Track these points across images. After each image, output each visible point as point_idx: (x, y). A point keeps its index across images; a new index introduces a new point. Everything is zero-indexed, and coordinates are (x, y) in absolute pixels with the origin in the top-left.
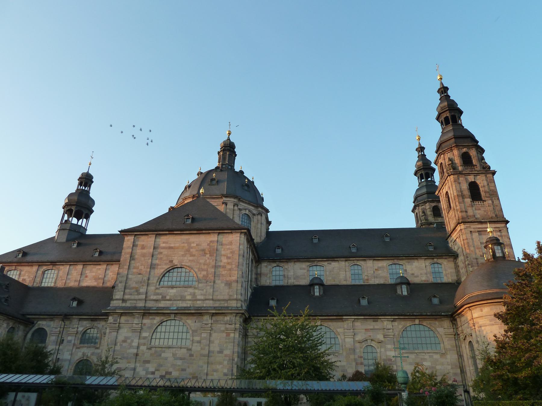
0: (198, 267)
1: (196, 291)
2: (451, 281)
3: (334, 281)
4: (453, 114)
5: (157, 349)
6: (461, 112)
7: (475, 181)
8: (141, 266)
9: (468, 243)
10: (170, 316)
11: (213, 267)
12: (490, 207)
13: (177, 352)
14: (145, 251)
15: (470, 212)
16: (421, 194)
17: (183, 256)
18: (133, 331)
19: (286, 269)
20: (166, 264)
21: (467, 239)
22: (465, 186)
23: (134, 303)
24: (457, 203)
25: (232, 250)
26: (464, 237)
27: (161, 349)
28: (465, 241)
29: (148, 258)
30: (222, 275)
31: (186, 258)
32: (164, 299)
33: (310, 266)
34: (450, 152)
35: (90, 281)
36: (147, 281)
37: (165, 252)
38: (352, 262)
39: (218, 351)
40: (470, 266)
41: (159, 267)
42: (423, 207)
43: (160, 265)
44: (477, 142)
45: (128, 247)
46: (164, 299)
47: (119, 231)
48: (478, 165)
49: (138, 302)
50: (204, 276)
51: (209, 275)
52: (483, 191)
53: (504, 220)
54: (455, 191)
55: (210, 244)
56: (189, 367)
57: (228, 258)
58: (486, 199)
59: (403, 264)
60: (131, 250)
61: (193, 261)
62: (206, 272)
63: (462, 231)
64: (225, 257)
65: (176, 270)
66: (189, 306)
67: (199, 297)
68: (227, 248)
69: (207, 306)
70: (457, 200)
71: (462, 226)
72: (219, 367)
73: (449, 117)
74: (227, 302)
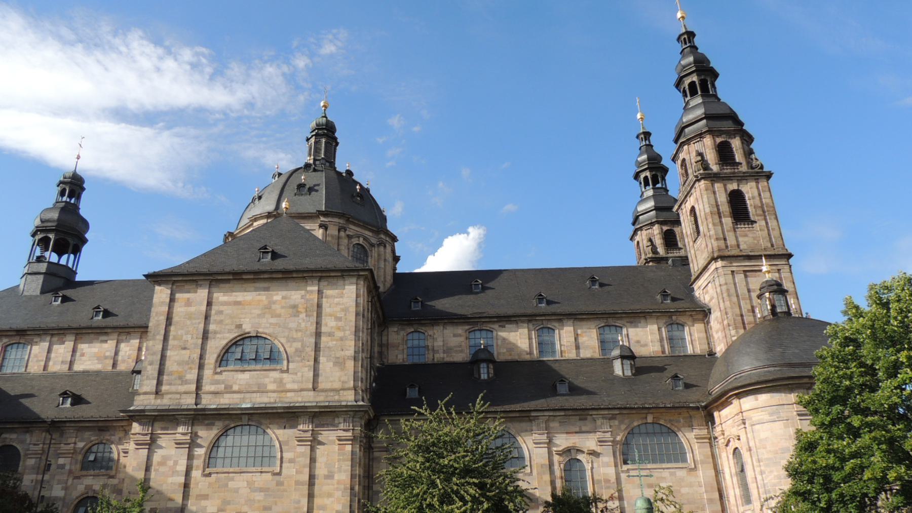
0: (286, 334)
1: (285, 375)
2: (699, 352)
3: (511, 355)
4: (703, 77)
5: (219, 475)
6: (715, 75)
7: (740, 188)
8: (186, 334)
9: (728, 290)
10: (241, 419)
11: (312, 336)
12: (763, 232)
13: (254, 479)
14: (192, 309)
17: (259, 316)
18: (178, 446)
19: (430, 336)
20: (230, 331)
21: (726, 284)
22: (723, 198)
23: (177, 399)
24: (711, 226)
25: (343, 306)
27: (226, 475)
28: (724, 288)
29: (197, 321)
30: (328, 347)
31: (264, 320)
32: (229, 390)
33: (470, 330)
34: (698, 141)
35: (89, 363)
36: (197, 361)
37: (227, 310)
38: (540, 323)
39: (325, 475)
40: (731, 328)
41: (218, 336)
42: (650, 231)
43: (220, 333)
44: (742, 124)
45: (163, 303)
46: (229, 390)
47: (144, 275)
48: (744, 163)
49: (184, 396)
50: (297, 350)
51: (306, 348)
52: (751, 205)
53: (785, 252)
54: (707, 206)
55: (306, 295)
56: (276, 504)
57: (338, 319)
58: (756, 218)
59: (621, 325)
60: (167, 308)
61: (276, 324)
62: (300, 344)
63: (719, 271)
64: (333, 318)
65: (247, 342)
66: (272, 400)
67: (289, 386)
68: (335, 302)
69: (304, 400)
70: (710, 220)
71: (720, 263)
72: (327, 501)
73: (697, 83)
74: (339, 393)
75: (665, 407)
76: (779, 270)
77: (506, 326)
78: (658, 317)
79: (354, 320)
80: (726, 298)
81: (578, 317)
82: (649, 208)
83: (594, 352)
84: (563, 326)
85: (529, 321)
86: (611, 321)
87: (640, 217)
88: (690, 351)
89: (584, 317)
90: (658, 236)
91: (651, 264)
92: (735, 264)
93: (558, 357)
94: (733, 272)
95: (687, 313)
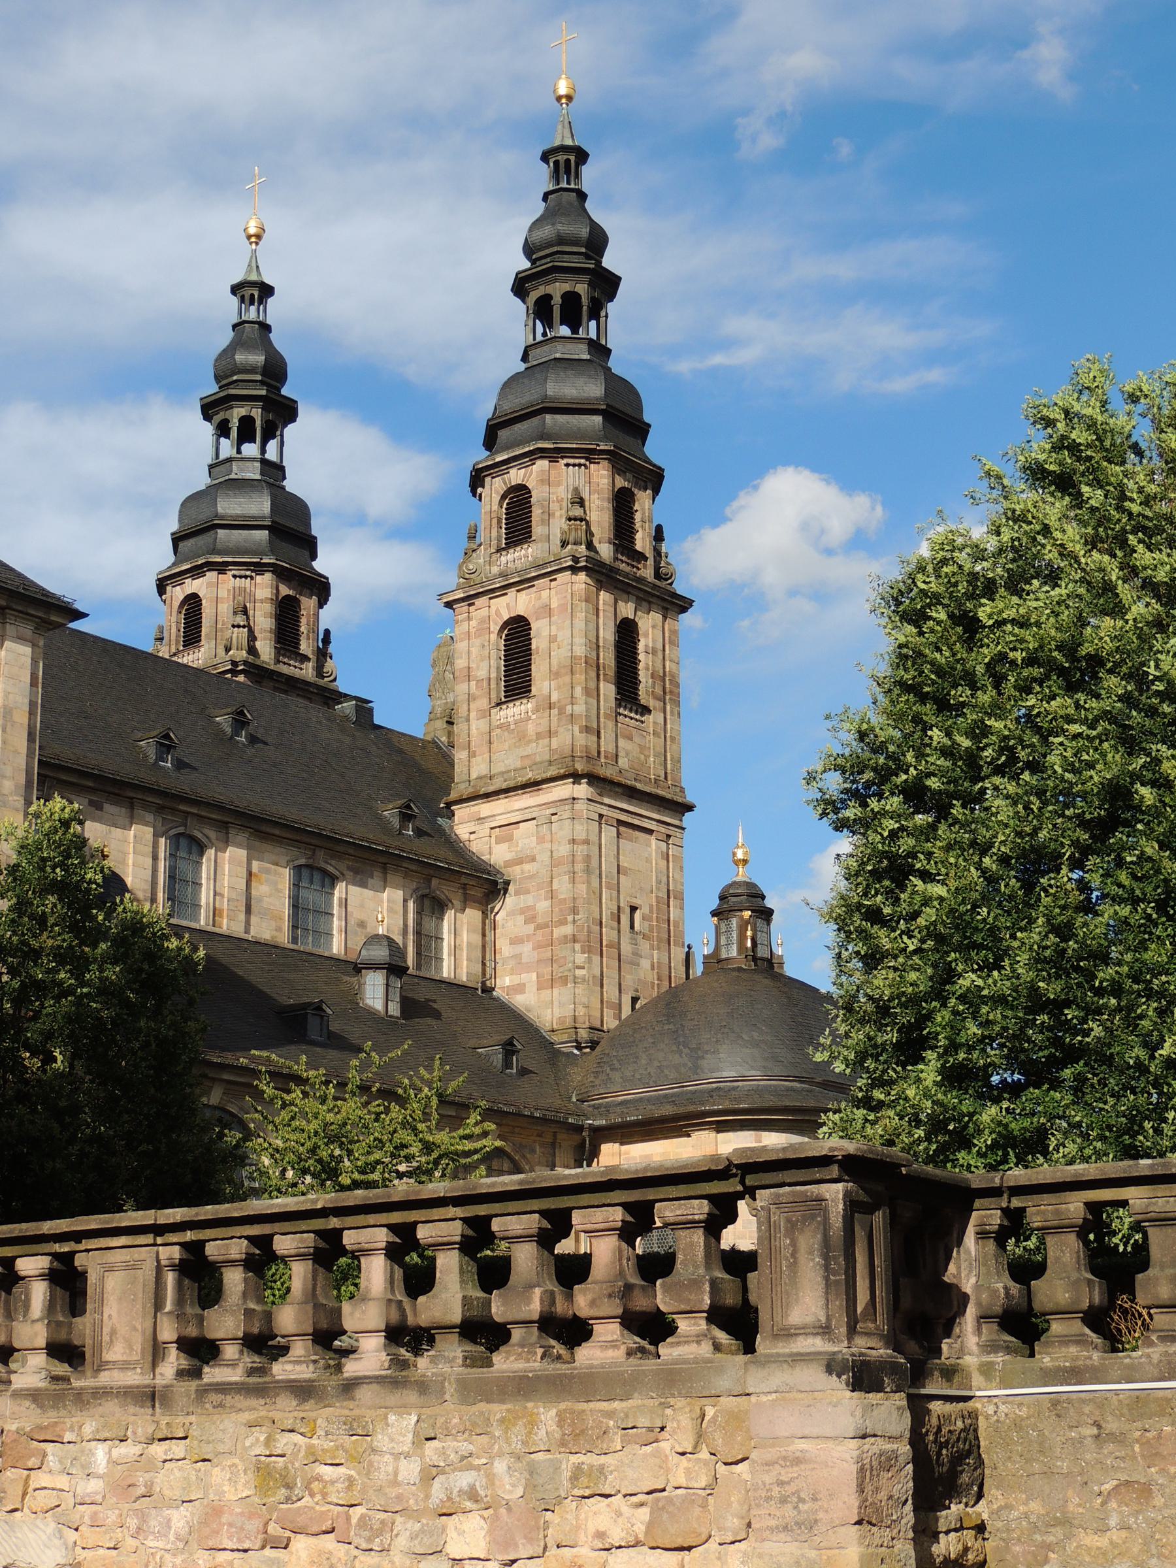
2: (465, 979)
6: (611, 296)
9: (588, 858)
16: (237, 517)
21: (587, 842)
22: (608, 635)
24: (578, 691)
26: (580, 830)
28: (581, 850)
34: (580, 465)
40: (578, 947)
48: (651, 562)
52: (647, 669)
54: (580, 640)
58: (652, 703)
59: (337, 873)
63: (577, 807)
70: (580, 677)
71: (583, 790)
75: (532, 1117)
76: (669, 836)
77: (106, 806)
78: (407, 874)
79: (24, 751)
81: (265, 828)
82: (255, 518)
83: (279, 929)
84: (227, 842)
87: (221, 533)
88: (445, 974)
89: (277, 832)
90: (268, 608)
91: (241, 678)
92: (607, 800)
93: (203, 922)
94: (601, 816)
95: (464, 880)
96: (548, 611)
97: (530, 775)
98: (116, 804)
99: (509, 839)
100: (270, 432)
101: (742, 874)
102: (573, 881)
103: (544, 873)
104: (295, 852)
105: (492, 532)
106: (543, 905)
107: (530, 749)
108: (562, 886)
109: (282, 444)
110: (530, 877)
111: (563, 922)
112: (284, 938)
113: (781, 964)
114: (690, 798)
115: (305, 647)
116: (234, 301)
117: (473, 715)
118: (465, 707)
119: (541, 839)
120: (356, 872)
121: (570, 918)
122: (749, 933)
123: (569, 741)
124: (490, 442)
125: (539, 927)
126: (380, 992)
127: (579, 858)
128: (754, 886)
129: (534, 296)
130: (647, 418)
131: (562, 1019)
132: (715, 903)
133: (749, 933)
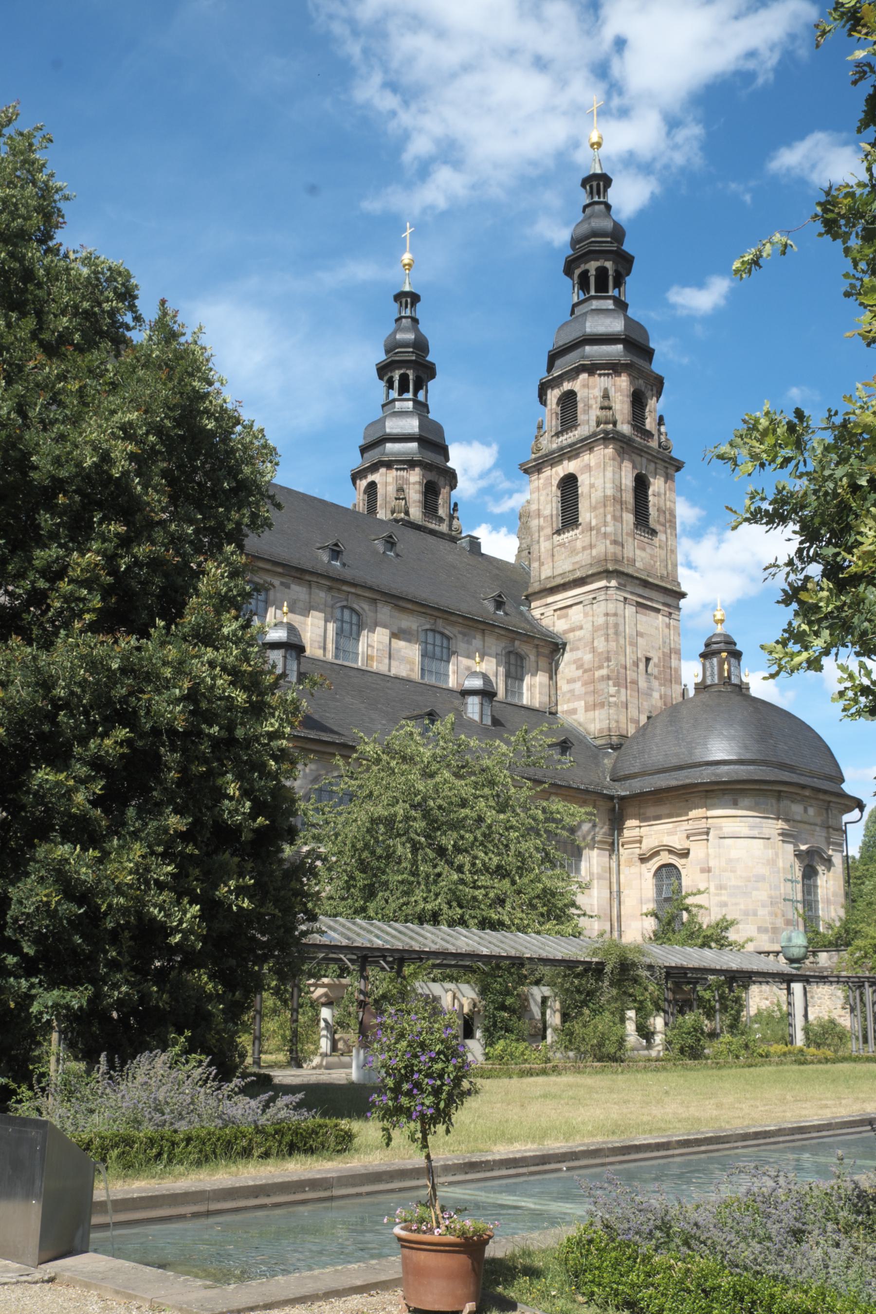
9: (616, 625)
15: (628, 552)
21: (615, 615)
22: (628, 481)
24: (609, 518)
26: (611, 607)
34: (608, 375)
38: (343, 596)
40: (611, 683)
48: (656, 437)
52: (654, 505)
54: (609, 485)
58: (658, 528)
70: (610, 509)
73: (611, 272)
75: (578, 789)
76: (670, 614)
77: (293, 586)
78: (499, 637)
80: (612, 636)
83: (412, 670)
85: (330, 589)
86: (440, 625)
88: (525, 701)
89: (410, 606)
94: (625, 599)
95: (536, 642)
96: (588, 468)
97: (578, 574)
98: (299, 585)
99: (566, 616)
100: (420, 385)
101: (719, 629)
102: (607, 640)
103: (588, 637)
104: (422, 620)
105: (551, 422)
106: (588, 657)
107: (578, 558)
108: (600, 644)
109: (427, 392)
110: (580, 640)
111: (601, 667)
112: (416, 676)
113: (748, 689)
114: (684, 589)
115: (442, 512)
116: (396, 306)
117: (542, 539)
118: (537, 534)
119: (586, 615)
120: (464, 635)
121: (605, 664)
122: (726, 667)
123: (603, 550)
124: (550, 367)
125: (585, 671)
126: (477, 708)
127: (610, 626)
128: (728, 636)
129: (577, 272)
130: (652, 345)
131: (601, 731)
132: (702, 649)
133: (726, 667)
